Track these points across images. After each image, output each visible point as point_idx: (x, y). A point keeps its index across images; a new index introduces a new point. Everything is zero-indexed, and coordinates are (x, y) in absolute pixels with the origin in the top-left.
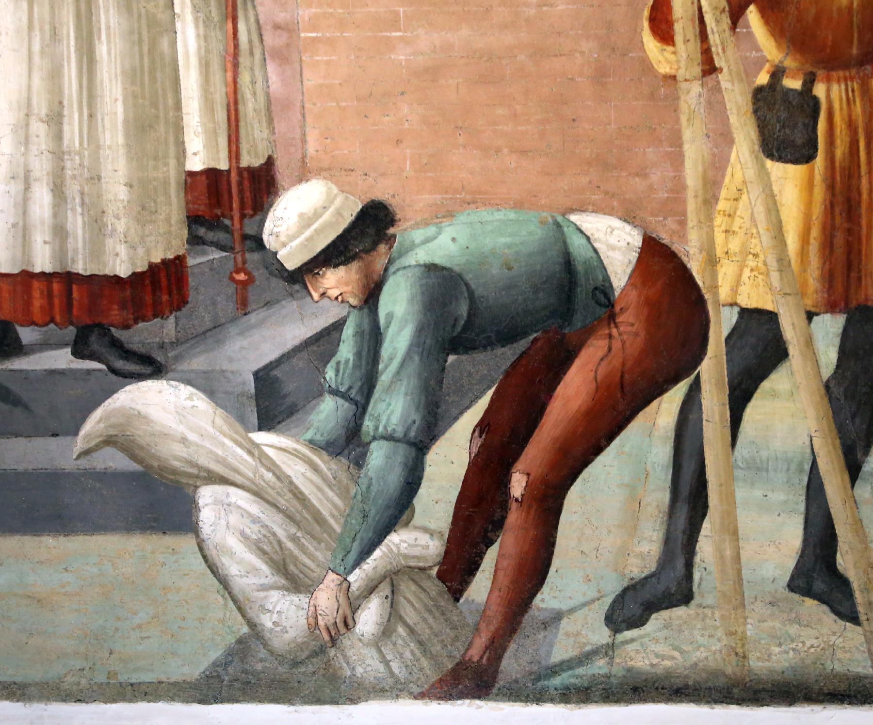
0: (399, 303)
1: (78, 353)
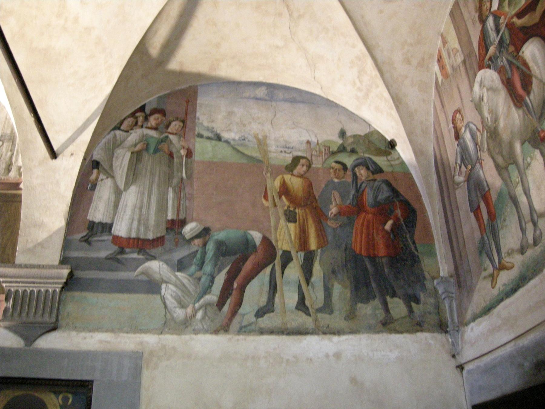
0: (211, 247)
1: (138, 254)
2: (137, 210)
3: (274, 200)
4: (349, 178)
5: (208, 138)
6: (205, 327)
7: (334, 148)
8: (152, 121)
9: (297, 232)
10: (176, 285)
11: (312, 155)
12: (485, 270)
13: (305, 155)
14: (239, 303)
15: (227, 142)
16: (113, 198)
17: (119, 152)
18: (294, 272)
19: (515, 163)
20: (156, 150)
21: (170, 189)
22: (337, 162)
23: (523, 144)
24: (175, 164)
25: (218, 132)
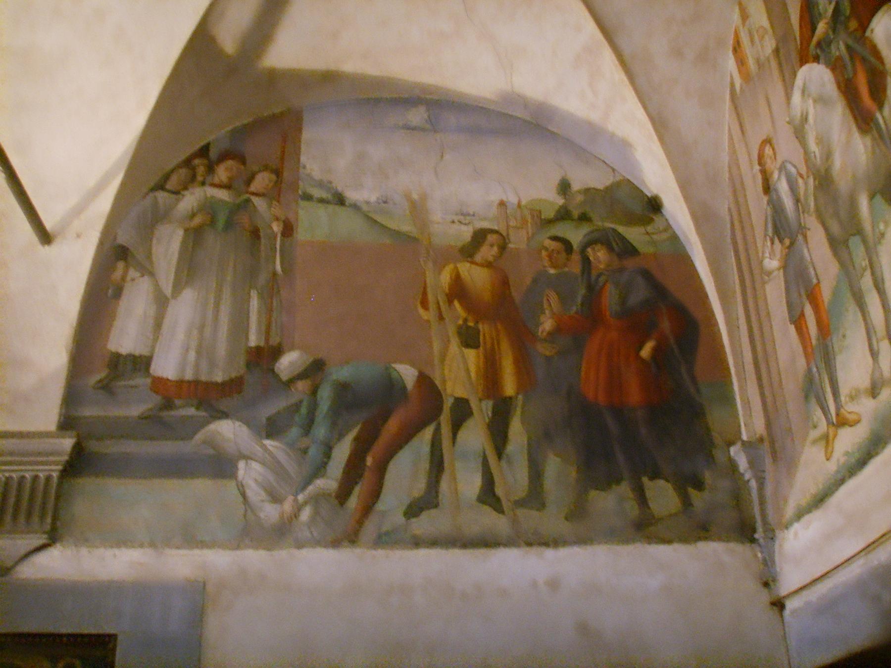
0: (325, 394)
1: (197, 409)
2: (195, 332)
3: (439, 308)
4: (575, 267)
5: (322, 201)
6: (315, 534)
7: (550, 214)
8: (222, 173)
9: (481, 364)
10: (263, 463)
11: (508, 226)
13: (496, 228)
14: (376, 493)
15: (355, 207)
16: (152, 311)
17: (163, 230)
18: (474, 436)
19: (859, 232)
20: (230, 225)
21: (254, 294)
22: (555, 238)
23: (872, 197)
24: (263, 248)
25: (340, 189)
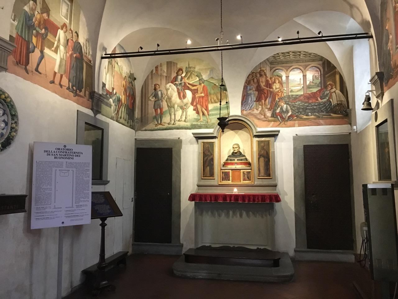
12: (154, 122)
19: (174, 108)
23: (178, 106)
